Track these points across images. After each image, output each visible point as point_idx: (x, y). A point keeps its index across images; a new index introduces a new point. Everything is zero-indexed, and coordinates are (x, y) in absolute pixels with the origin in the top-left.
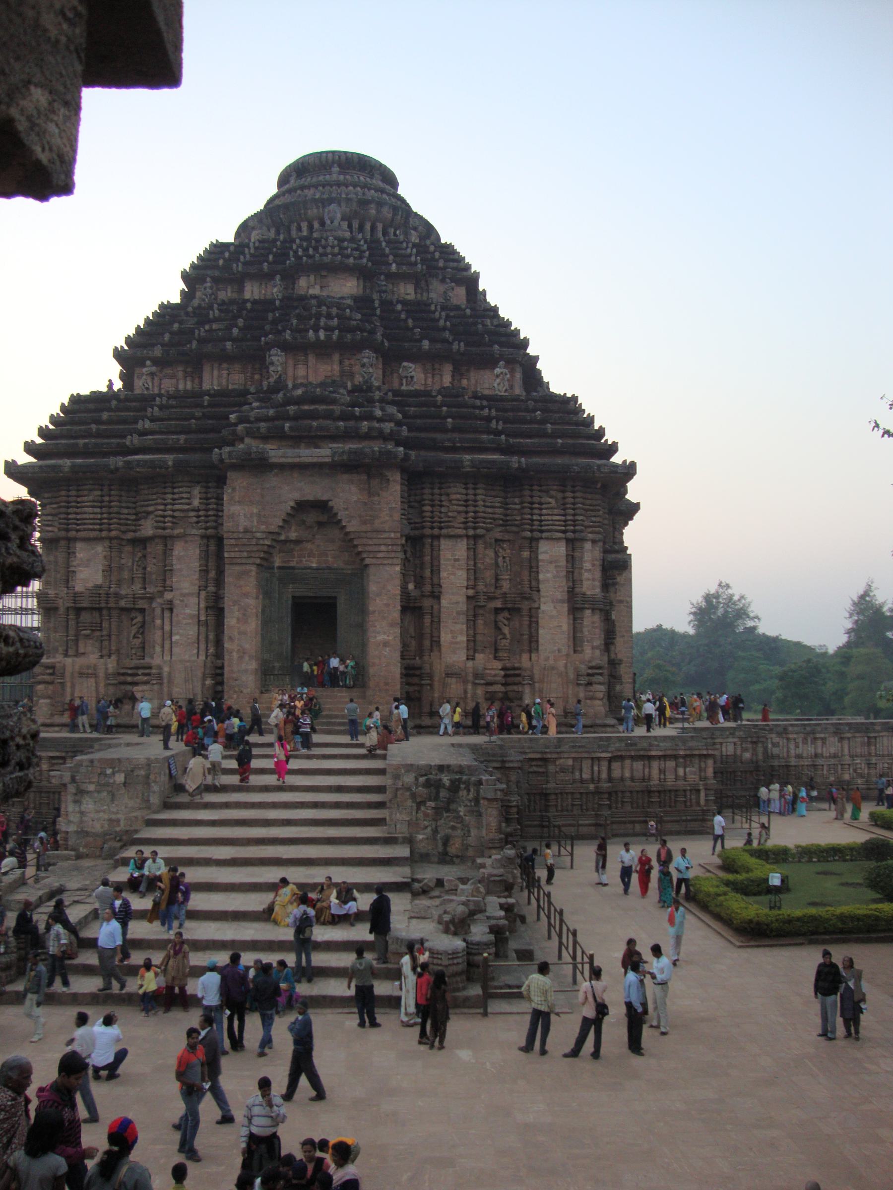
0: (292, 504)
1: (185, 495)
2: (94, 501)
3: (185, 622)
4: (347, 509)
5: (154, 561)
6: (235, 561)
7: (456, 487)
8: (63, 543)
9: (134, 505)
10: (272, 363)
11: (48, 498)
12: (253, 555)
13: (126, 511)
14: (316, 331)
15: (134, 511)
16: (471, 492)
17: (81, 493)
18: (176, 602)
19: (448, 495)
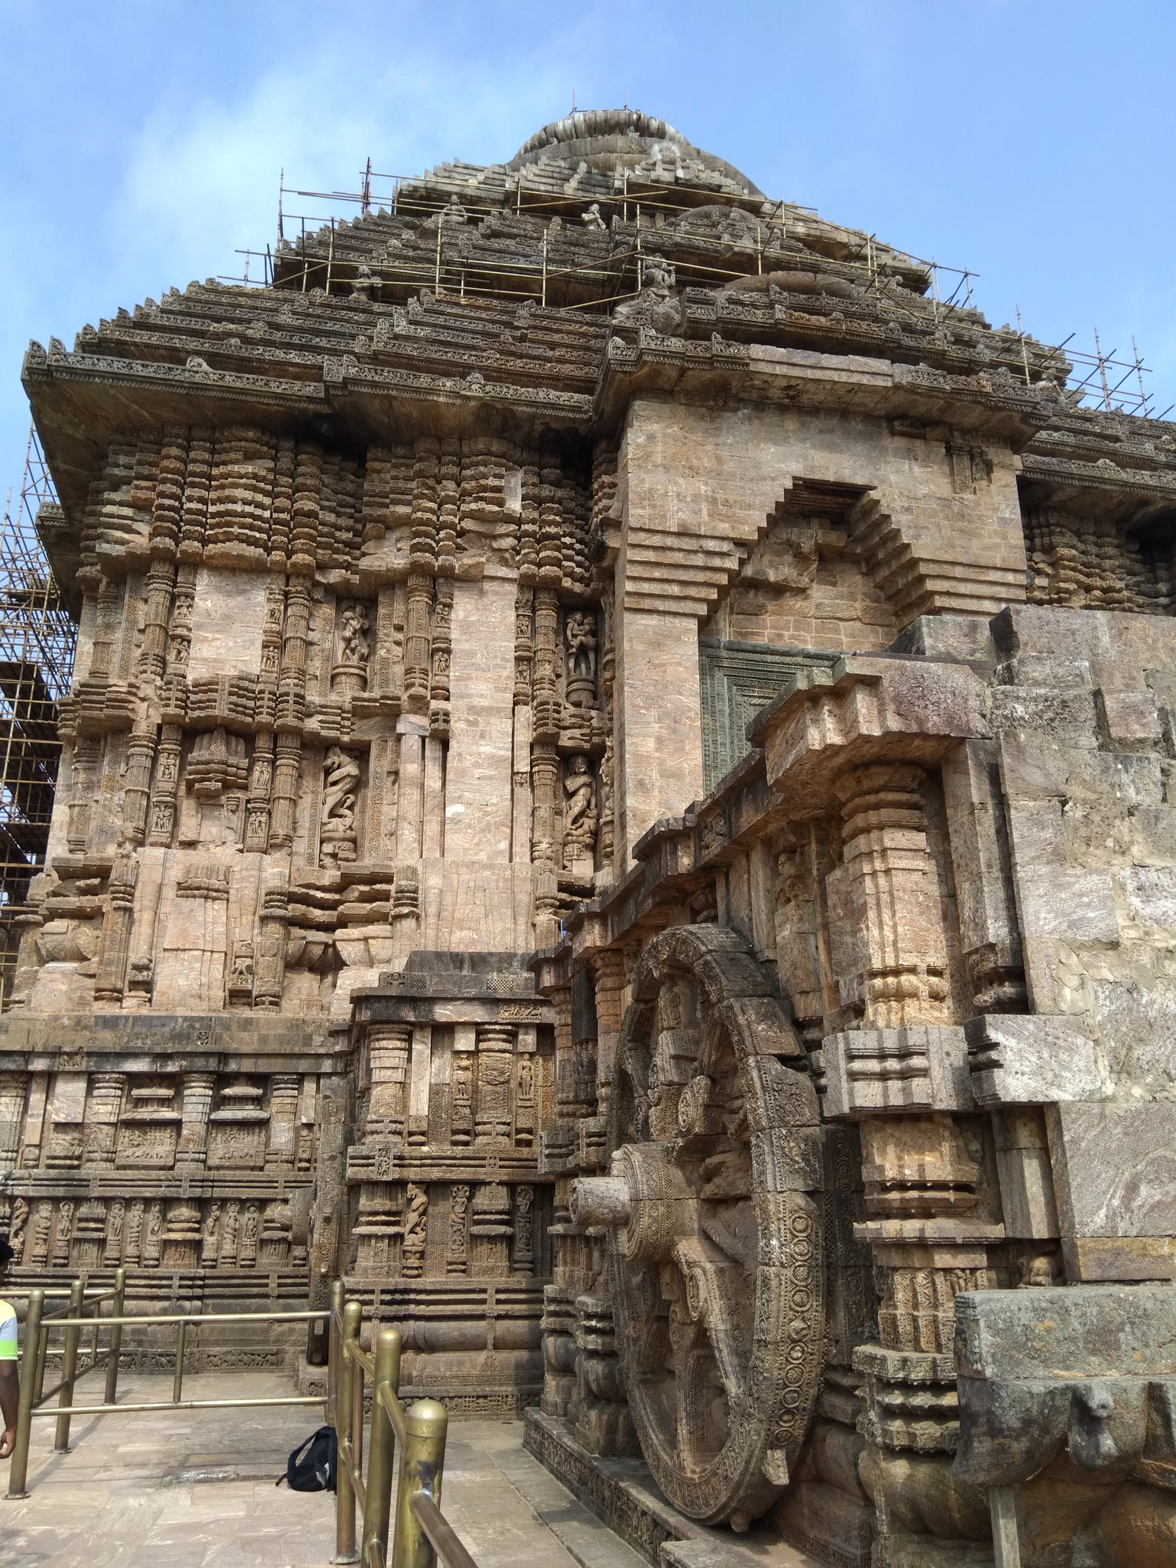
0: (789, 484)
1: (492, 482)
2: (255, 476)
3: (478, 772)
4: (908, 510)
5: (400, 636)
6: (647, 604)
7: (1062, 534)
8: (158, 569)
9: (348, 510)
10: (649, 282)
11: (127, 467)
12: (693, 592)
13: (331, 518)
14: (736, 237)
15: (351, 522)
16: (1093, 549)
17: (217, 458)
18: (457, 726)
19: (1049, 550)
